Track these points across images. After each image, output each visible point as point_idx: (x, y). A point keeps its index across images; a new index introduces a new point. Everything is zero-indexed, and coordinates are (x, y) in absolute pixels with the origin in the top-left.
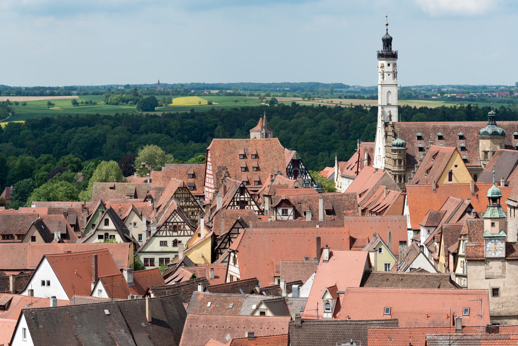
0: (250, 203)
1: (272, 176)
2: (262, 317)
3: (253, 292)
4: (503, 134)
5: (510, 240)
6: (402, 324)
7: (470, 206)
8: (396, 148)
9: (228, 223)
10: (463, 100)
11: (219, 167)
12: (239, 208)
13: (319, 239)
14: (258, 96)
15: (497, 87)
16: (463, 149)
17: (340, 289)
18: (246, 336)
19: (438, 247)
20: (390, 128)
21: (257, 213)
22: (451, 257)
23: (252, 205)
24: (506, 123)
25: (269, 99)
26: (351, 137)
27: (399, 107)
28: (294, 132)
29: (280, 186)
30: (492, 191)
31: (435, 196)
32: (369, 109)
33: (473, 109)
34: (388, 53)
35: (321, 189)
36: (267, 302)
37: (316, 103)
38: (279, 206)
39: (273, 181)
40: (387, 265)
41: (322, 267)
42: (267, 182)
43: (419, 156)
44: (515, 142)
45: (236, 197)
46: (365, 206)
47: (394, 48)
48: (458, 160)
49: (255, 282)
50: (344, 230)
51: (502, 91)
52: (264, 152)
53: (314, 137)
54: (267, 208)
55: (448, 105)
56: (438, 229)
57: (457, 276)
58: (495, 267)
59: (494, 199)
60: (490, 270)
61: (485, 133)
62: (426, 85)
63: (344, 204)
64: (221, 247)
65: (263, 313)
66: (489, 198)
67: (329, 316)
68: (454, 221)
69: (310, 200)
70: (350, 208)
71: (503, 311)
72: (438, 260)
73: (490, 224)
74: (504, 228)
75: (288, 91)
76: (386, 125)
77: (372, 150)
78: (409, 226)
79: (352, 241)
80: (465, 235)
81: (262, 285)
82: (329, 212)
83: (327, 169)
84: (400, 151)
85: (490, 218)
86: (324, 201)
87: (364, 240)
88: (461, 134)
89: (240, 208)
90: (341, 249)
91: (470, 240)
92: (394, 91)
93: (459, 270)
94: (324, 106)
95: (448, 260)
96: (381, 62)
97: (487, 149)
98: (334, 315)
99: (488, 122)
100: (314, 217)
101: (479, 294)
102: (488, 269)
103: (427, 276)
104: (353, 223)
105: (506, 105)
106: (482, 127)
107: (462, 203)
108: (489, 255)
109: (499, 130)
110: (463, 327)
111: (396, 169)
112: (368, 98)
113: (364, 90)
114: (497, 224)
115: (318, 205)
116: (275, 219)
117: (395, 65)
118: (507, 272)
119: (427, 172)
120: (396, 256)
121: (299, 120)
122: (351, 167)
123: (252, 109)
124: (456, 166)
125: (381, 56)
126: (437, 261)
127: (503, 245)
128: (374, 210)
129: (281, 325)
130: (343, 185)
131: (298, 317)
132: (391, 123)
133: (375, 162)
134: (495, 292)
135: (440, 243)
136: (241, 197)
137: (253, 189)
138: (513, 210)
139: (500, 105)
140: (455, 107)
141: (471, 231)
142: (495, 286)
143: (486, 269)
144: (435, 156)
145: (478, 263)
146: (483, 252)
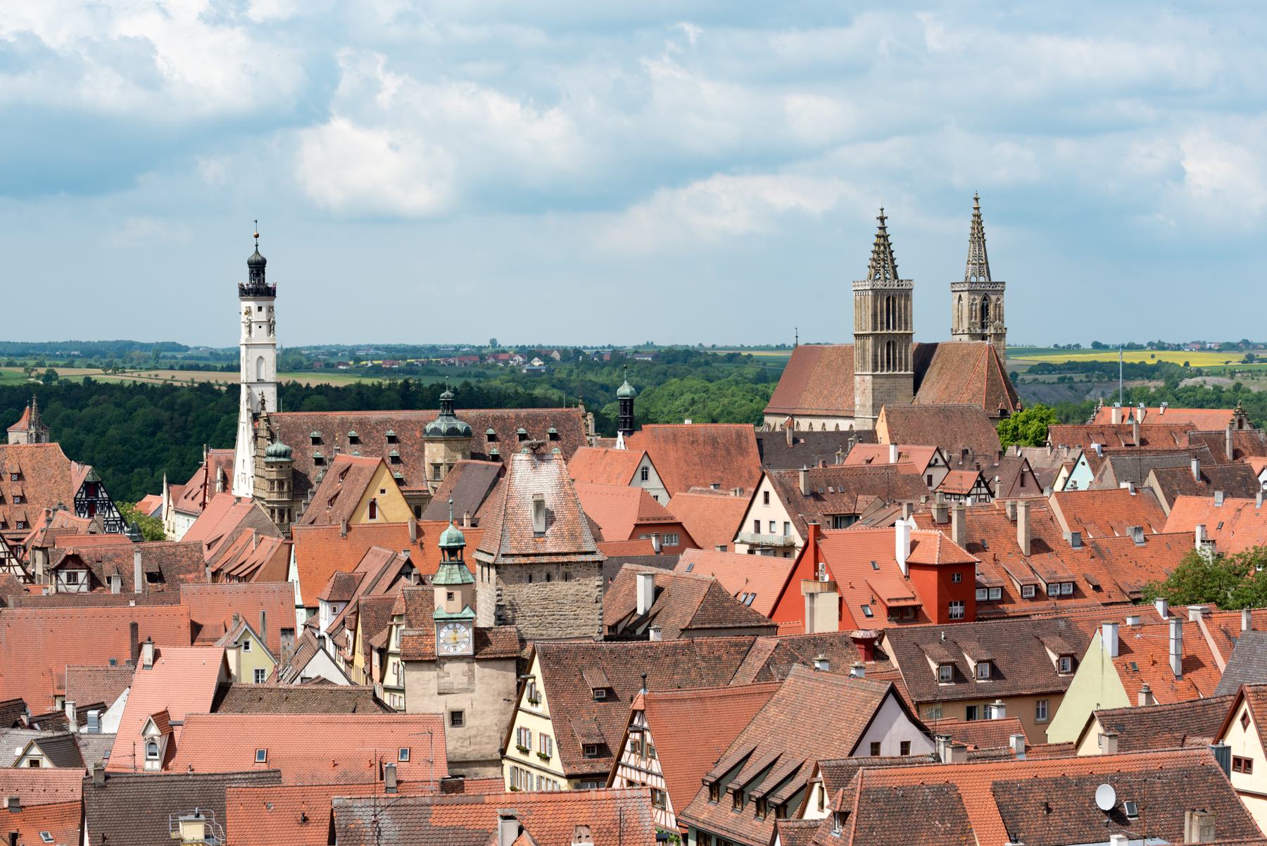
1: (48, 512)
2: (34, 770)
3: (16, 725)
4: (468, 433)
5: (482, 623)
6: (288, 779)
7: (409, 563)
8: (273, 459)
13: (134, 627)
15: (457, 348)
16: (396, 460)
17: (175, 717)
18: (6, 804)
19: (351, 638)
20: (262, 424)
21: (21, 580)
22: (376, 656)
24: (472, 413)
25: (43, 371)
26: (192, 440)
27: (279, 385)
28: (89, 431)
29: (63, 531)
30: (446, 536)
31: (344, 545)
32: (224, 389)
33: (413, 389)
34: (259, 287)
35: (138, 535)
36: (41, 743)
37: (128, 378)
38: (62, 566)
39: (49, 521)
40: (259, 673)
41: (140, 677)
42: (39, 524)
43: (315, 473)
46: (218, 565)
47: (269, 280)
48: (386, 481)
49: (20, 706)
50: (181, 609)
51: (466, 354)
53: (124, 441)
54: (39, 569)
55: (367, 381)
56: (351, 605)
57: (387, 689)
58: (455, 671)
59: (452, 551)
61: (436, 431)
62: (327, 344)
65: (35, 763)
66: (443, 549)
67: (155, 766)
68: (379, 591)
69: (118, 556)
71: (471, 752)
73: (445, 596)
74: (470, 602)
75: (78, 356)
76: (255, 417)
77: (230, 463)
78: (299, 601)
79: (196, 629)
80: (400, 616)
81: (32, 711)
82: (153, 577)
83: (149, 498)
84: (280, 465)
85: (445, 585)
86: (144, 556)
87: (217, 628)
88: (391, 433)
90: (174, 643)
91: (410, 625)
92: (270, 356)
93: (391, 680)
94: (143, 385)
95: (369, 660)
96: (245, 304)
97: (439, 461)
98: (165, 765)
99: (439, 412)
100: (126, 587)
101: (427, 721)
103: (331, 691)
104: (197, 598)
105: (473, 381)
107: (394, 557)
108: (444, 651)
109: (460, 426)
110: (399, 782)
111: (274, 497)
112: (223, 370)
113: (215, 355)
114: (458, 594)
117: (271, 309)
119: (331, 502)
120: (275, 655)
121: (97, 410)
122: (192, 495)
123: (12, 389)
125: (244, 292)
126: (350, 663)
127: (466, 634)
128: (234, 573)
129: (67, 783)
130: (178, 528)
131: (99, 770)
132: (264, 414)
133: (235, 486)
134: (457, 718)
135: (355, 630)
137: (14, 537)
138: (486, 569)
139: (462, 380)
140: (380, 384)
141: (411, 608)
142: (456, 707)
144: (344, 474)
145: (425, 666)
146: (433, 646)
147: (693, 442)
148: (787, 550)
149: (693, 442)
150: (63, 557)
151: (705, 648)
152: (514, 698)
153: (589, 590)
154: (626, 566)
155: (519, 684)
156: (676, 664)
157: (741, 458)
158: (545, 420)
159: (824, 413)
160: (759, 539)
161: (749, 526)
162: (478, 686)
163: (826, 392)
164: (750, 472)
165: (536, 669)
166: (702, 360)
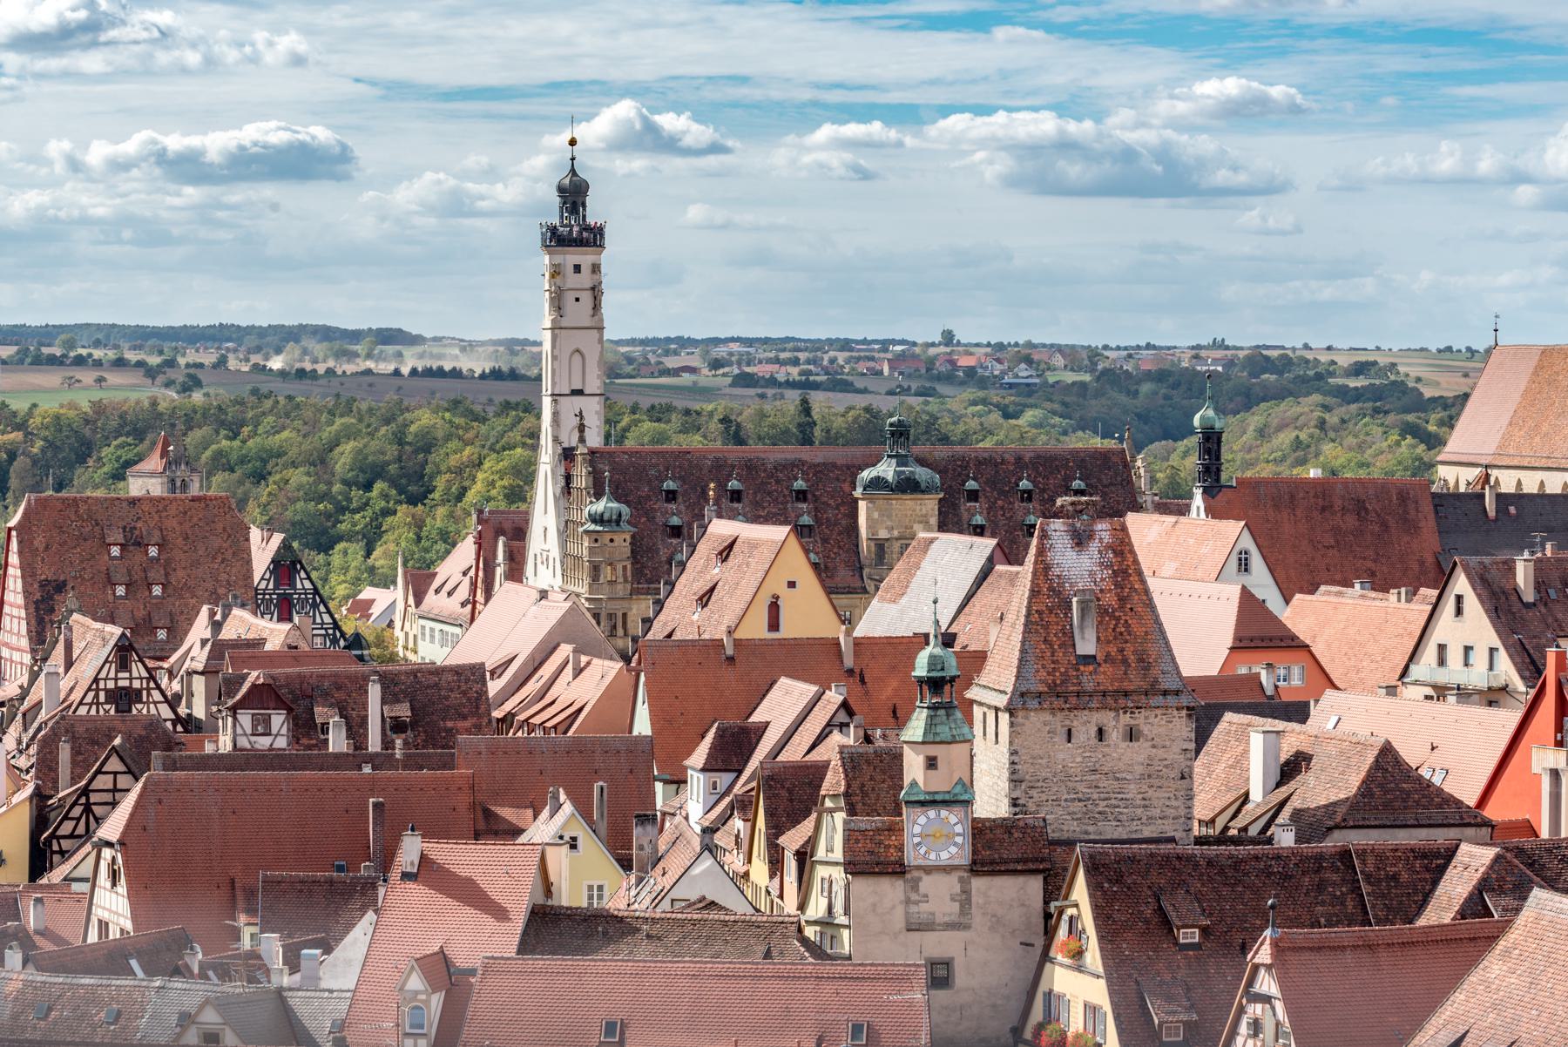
0: (149, 694)
9: (80, 758)
10: (780, 385)
11: (44, 584)
12: (112, 712)
14: (140, 364)
21: (169, 724)
22: (791, 865)
23: (155, 703)
44: (968, 510)
45: (103, 675)
51: (901, 357)
52: (187, 538)
60: (924, 907)
63: (447, 698)
64: (59, 833)
66: (921, 681)
68: (794, 753)
70: (465, 711)
72: (746, 875)
76: (568, 455)
88: (799, 484)
89: (117, 711)
91: (852, 811)
97: (883, 534)
102: (917, 903)
106: (868, 466)
115: (365, 706)
116: (229, 747)
118: (974, 910)
122: (448, 587)
124: (792, 584)
128: (536, 720)
136: (120, 675)
141: (856, 784)
143: (908, 902)
144: (726, 552)
146: (901, 849)
147: (1324, 509)
148: (1494, 696)
149: (1324, 509)
150: (244, 689)
151: (1371, 861)
152: (1040, 942)
153: (1170, 757)
154: (1229, 716)
155: (1048, 916)
156: (1320, 887)
157: (1407, 538)
158: (1066, 467)
159: (1543, 463)
160: (1442, 677)
161: (1429, 654)
162: (977, 919)
163: (1545, 428)
164: (1422, 563)
165: (1080, 891)
166: (1311, 373)
